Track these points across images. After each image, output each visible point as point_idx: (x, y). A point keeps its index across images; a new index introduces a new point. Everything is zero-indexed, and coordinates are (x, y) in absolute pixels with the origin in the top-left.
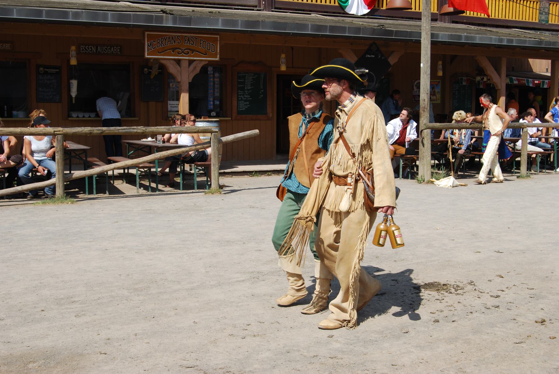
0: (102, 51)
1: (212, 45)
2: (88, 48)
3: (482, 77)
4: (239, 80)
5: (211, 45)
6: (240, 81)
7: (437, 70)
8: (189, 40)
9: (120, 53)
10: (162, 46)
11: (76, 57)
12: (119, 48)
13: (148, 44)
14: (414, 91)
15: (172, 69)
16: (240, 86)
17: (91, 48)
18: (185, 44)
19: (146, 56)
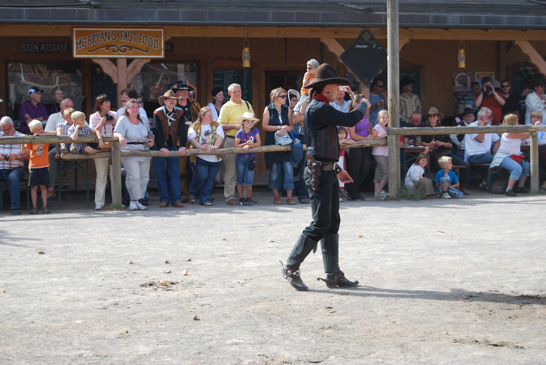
0: (46, 50)
1: (155, 40)
2: (30, 47)
5: (153, 41)
6: (217, 79)
7: (458, 61)
8: (126, 36)
9: (67, 51)
10: (93, 43)
12: (67, 45)
13: (77, 41)
14: (456, 86)
15: (108, 69)
16: (218, 86)
17: (33, 46)
18: (121, 40)
19: (75, 56)
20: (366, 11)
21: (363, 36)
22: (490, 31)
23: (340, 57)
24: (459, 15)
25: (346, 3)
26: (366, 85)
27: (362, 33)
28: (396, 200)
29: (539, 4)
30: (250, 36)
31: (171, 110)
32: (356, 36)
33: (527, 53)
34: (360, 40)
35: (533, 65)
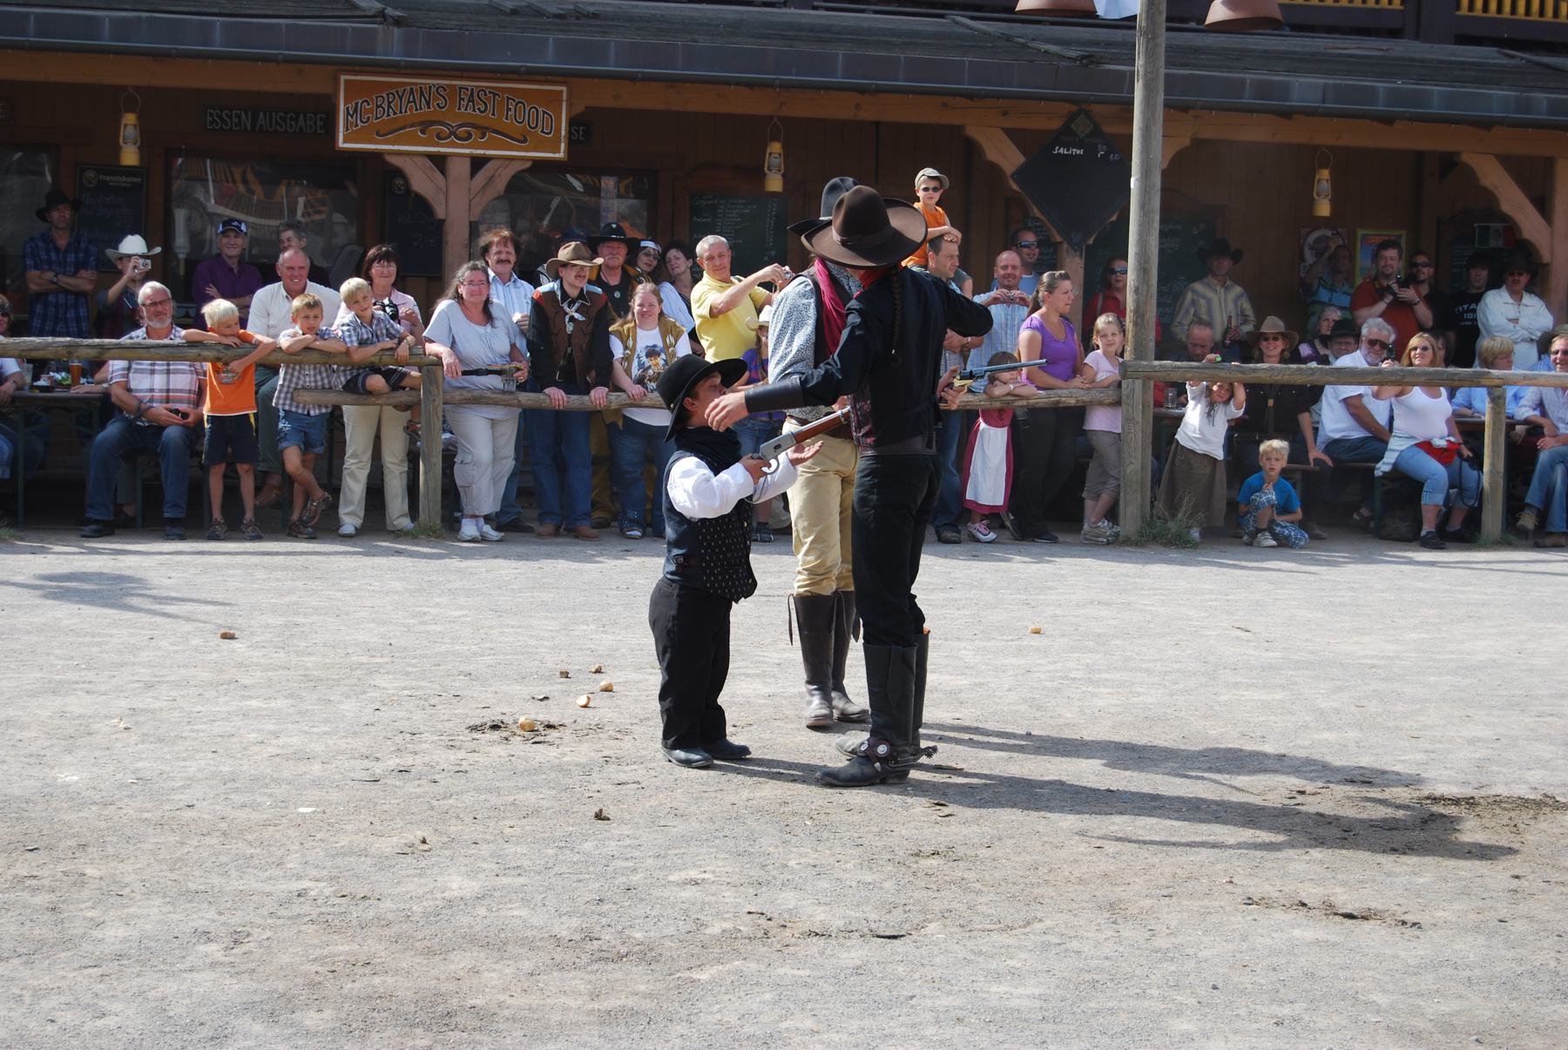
0: (271, 127)
2: (230, 117)
4: (695, 218)
5: (541, 114)
7: (1314, 199)
8: (471, 100)
9: (323, 132)
10: (388, 115)
11: (138, 144)
12: (324, 116)
13: (348, 108)
15: (422, 181)
17: (239, 116)
18: (459, 109)
19: (342, 144)
20: (1084, 61)
21: (1073, 126)
22: (1398, 125)
23: (1012, 176)
24: (1320, 81)
25: (1033, 40)
26: (1076, 251)
27: (1072, 117)
28: (1136, 545)
29: (1529, 61)
31: (573, 293)
32: (1056, 124)
33: (1490, 187)
34: (1065, 135)
35: (1505, 218)
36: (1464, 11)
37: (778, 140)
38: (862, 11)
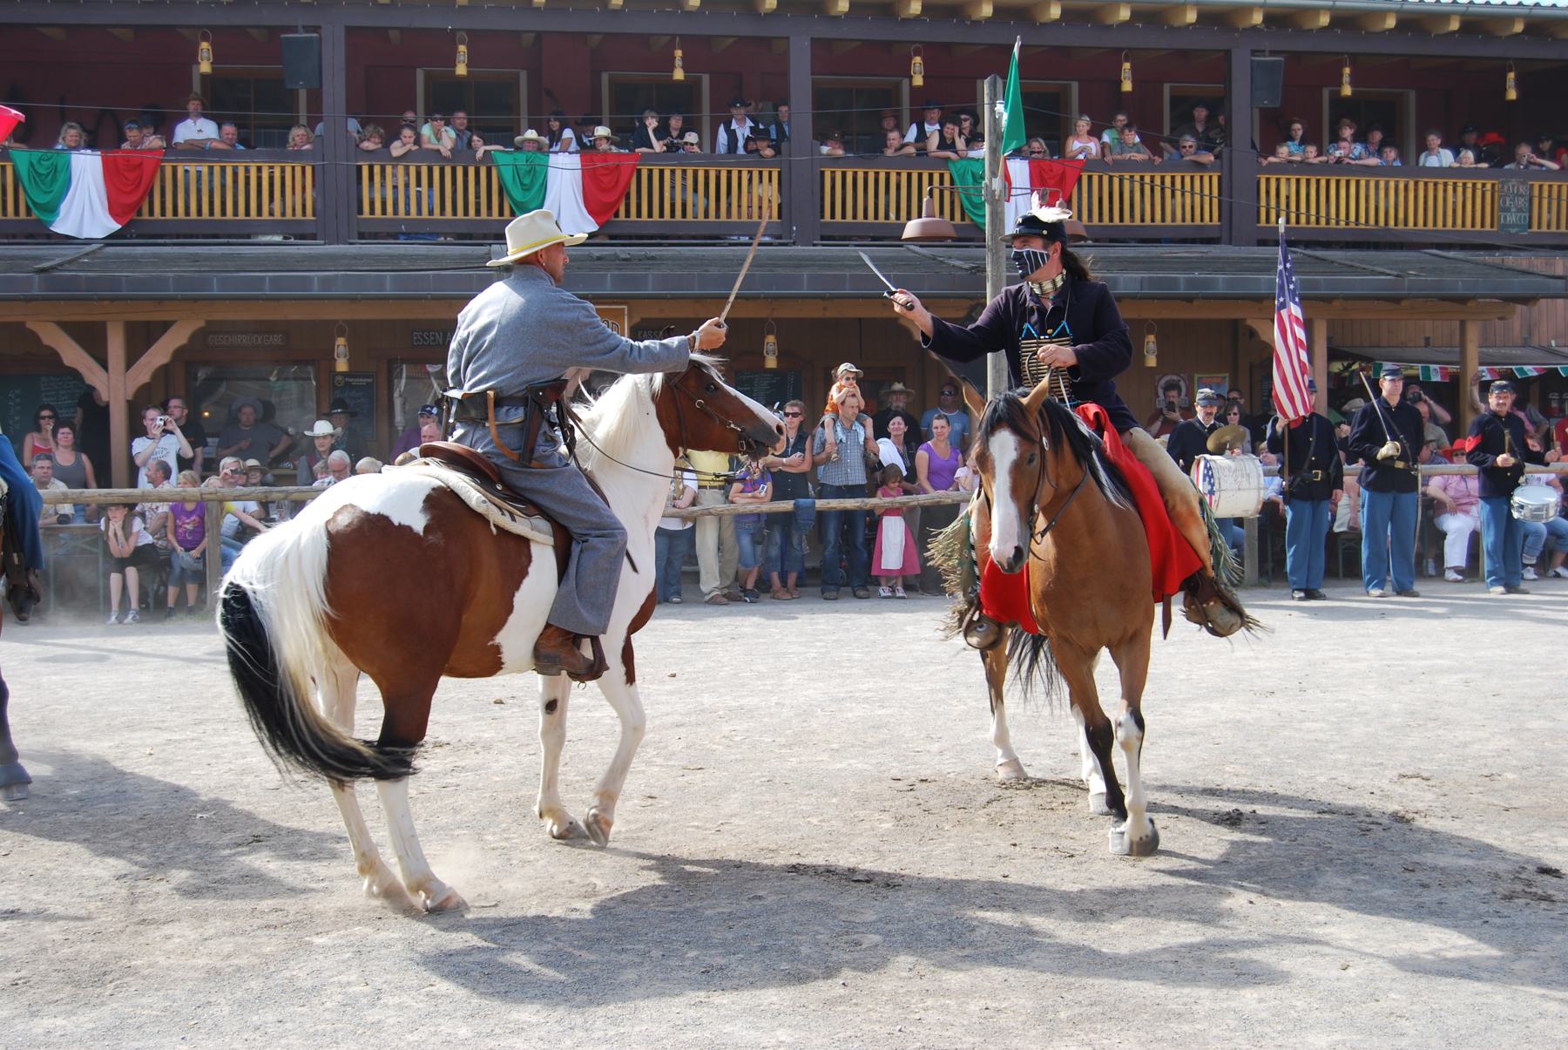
3: (1346, 364)
17: (434, 336)
25: (950, 258)
29: (1304, 254)
30: (776, 315)
36: (1263, 223)
37: (772, 334)
38: (847, 245)
